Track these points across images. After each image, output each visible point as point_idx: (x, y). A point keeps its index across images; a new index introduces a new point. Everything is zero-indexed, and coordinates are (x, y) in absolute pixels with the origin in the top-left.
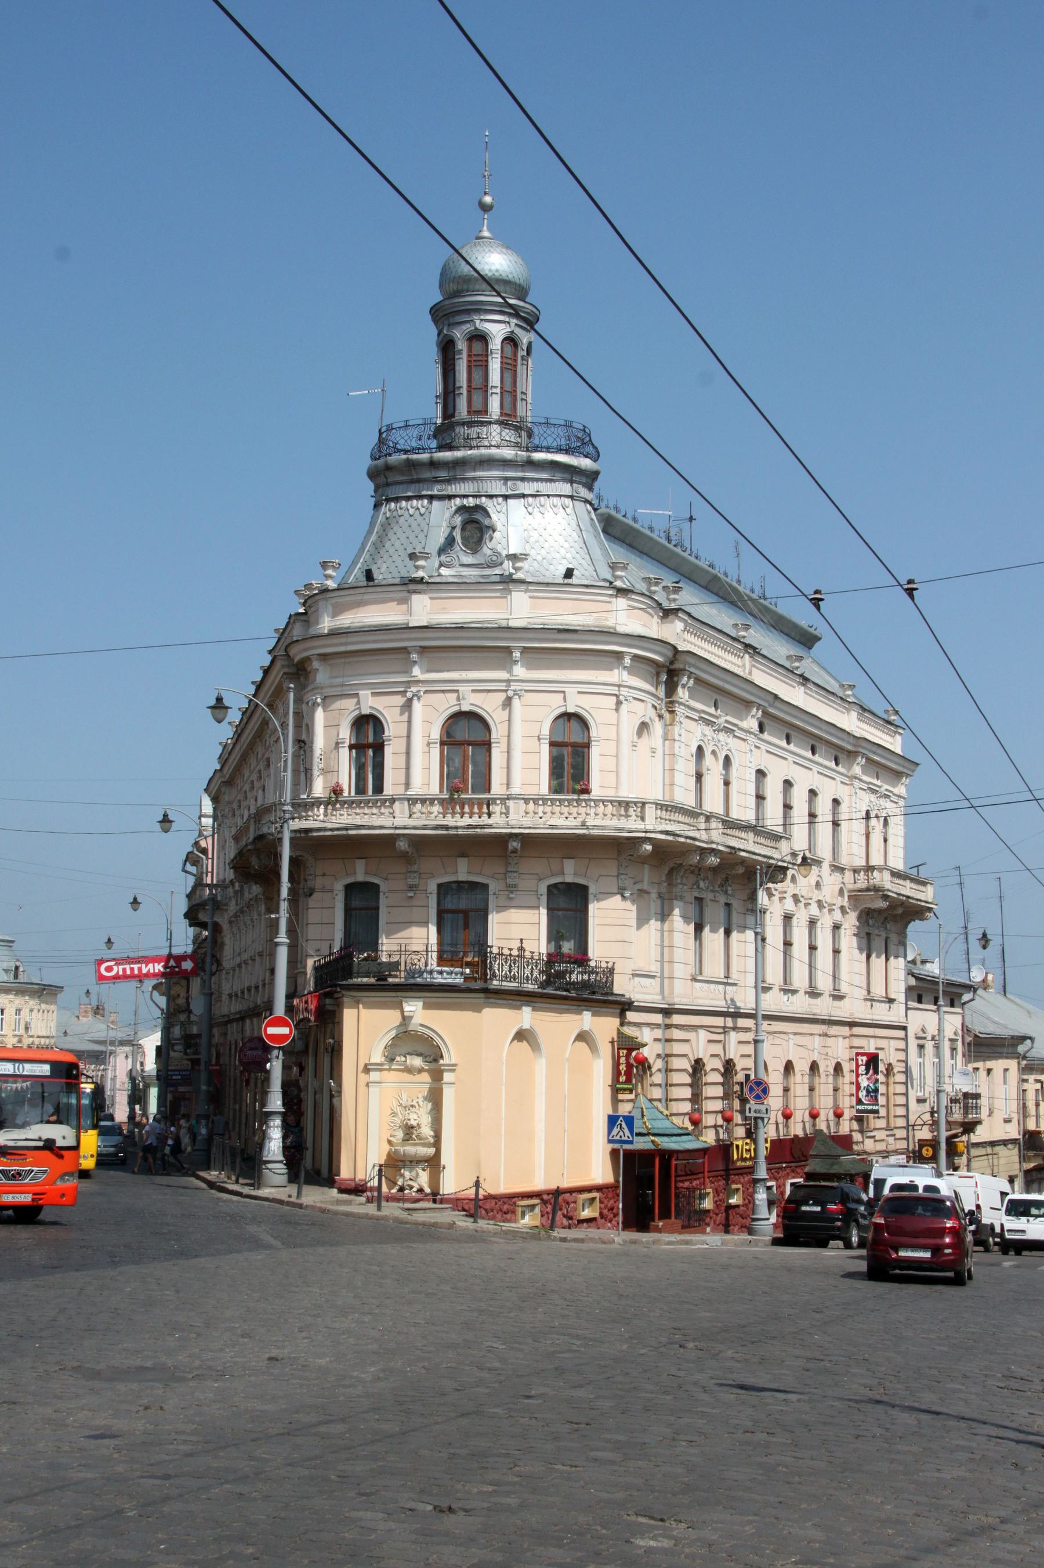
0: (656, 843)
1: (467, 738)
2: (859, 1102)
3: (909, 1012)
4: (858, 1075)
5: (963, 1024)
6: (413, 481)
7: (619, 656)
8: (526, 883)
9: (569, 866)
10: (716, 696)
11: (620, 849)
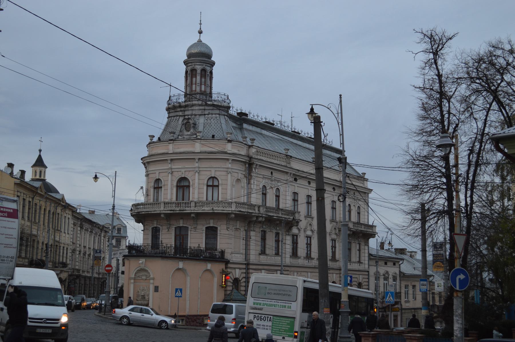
0: (235, 214)
1: (183, 185)
3: (370, 267)
6: (175, 112)
7: (228, 159)
8: (199, 227)
9: (212, 221)
10: (271, 171)
11: (225, 216)
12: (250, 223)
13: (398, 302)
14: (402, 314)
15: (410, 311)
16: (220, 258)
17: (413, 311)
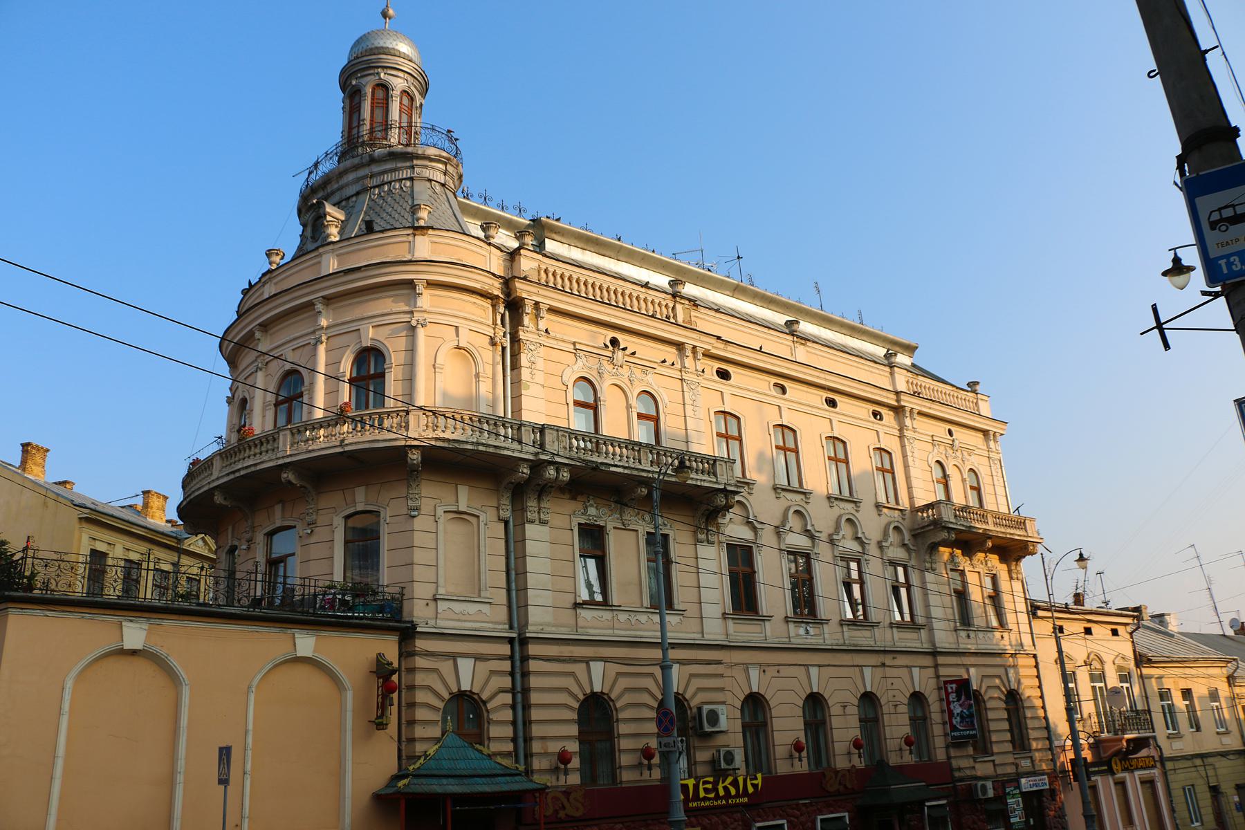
2: (954, 728)
4: (949, 703)
5: (1134, 651)
12: (519, 493)
13: (1147, 739)
14: (1165, 774)
15: (1188, 763)
16: (391, 617)
17: (1198, 762)
